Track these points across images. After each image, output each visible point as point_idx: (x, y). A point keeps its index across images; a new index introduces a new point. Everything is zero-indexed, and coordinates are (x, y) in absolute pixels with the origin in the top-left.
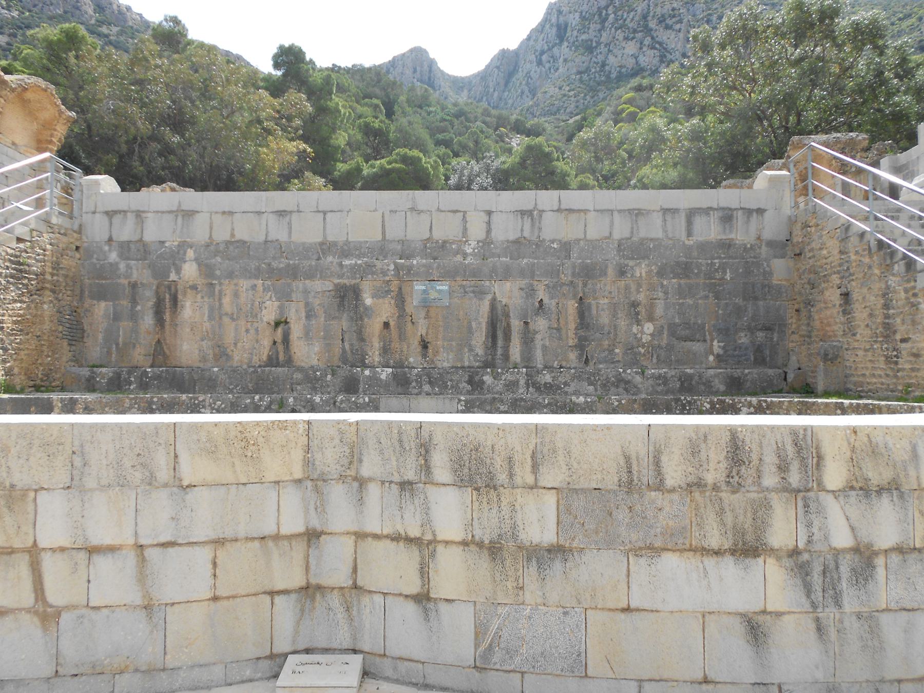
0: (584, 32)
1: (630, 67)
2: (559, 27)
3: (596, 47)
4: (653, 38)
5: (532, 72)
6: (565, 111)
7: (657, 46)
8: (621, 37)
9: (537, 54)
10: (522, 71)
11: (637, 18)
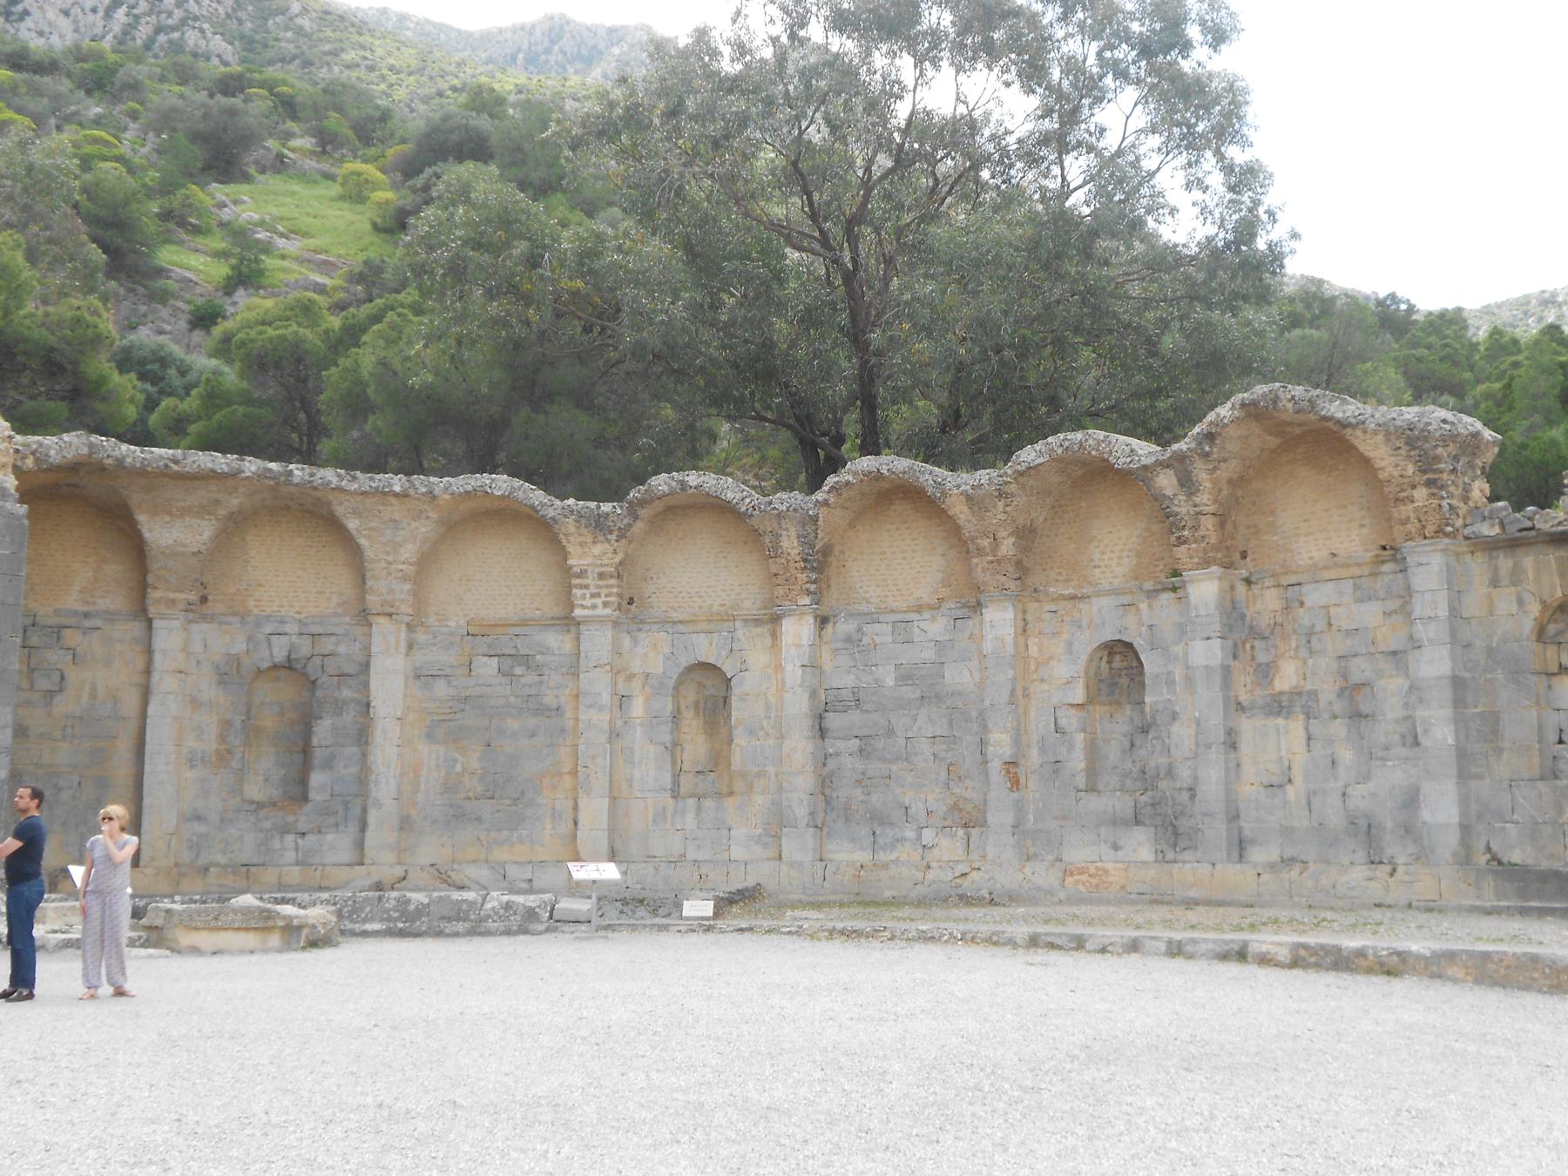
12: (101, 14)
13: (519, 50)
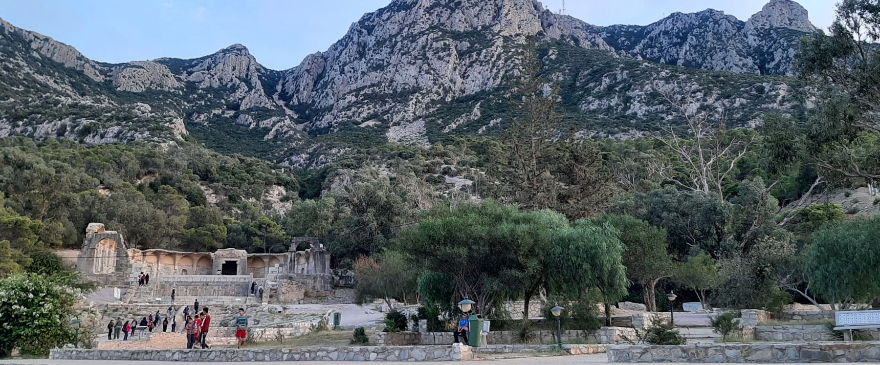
0: (378, 53)
1: (412, 86)
2: (359, 44)
3: (387, 66)
4: (429, 65)
5: (335, 79)
6: (359, 115)
7: (432, 72)
8: (405, 62)
9: (340, 64)
10: (329, 76)
11: (418, 48)
12: (489, 70)
13: (661, 31)
